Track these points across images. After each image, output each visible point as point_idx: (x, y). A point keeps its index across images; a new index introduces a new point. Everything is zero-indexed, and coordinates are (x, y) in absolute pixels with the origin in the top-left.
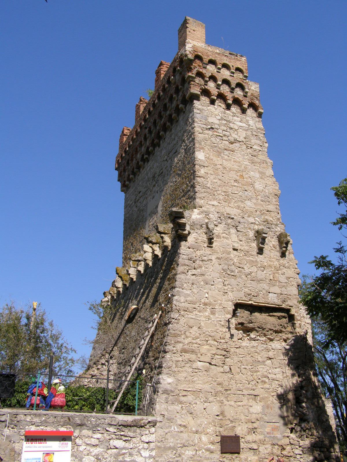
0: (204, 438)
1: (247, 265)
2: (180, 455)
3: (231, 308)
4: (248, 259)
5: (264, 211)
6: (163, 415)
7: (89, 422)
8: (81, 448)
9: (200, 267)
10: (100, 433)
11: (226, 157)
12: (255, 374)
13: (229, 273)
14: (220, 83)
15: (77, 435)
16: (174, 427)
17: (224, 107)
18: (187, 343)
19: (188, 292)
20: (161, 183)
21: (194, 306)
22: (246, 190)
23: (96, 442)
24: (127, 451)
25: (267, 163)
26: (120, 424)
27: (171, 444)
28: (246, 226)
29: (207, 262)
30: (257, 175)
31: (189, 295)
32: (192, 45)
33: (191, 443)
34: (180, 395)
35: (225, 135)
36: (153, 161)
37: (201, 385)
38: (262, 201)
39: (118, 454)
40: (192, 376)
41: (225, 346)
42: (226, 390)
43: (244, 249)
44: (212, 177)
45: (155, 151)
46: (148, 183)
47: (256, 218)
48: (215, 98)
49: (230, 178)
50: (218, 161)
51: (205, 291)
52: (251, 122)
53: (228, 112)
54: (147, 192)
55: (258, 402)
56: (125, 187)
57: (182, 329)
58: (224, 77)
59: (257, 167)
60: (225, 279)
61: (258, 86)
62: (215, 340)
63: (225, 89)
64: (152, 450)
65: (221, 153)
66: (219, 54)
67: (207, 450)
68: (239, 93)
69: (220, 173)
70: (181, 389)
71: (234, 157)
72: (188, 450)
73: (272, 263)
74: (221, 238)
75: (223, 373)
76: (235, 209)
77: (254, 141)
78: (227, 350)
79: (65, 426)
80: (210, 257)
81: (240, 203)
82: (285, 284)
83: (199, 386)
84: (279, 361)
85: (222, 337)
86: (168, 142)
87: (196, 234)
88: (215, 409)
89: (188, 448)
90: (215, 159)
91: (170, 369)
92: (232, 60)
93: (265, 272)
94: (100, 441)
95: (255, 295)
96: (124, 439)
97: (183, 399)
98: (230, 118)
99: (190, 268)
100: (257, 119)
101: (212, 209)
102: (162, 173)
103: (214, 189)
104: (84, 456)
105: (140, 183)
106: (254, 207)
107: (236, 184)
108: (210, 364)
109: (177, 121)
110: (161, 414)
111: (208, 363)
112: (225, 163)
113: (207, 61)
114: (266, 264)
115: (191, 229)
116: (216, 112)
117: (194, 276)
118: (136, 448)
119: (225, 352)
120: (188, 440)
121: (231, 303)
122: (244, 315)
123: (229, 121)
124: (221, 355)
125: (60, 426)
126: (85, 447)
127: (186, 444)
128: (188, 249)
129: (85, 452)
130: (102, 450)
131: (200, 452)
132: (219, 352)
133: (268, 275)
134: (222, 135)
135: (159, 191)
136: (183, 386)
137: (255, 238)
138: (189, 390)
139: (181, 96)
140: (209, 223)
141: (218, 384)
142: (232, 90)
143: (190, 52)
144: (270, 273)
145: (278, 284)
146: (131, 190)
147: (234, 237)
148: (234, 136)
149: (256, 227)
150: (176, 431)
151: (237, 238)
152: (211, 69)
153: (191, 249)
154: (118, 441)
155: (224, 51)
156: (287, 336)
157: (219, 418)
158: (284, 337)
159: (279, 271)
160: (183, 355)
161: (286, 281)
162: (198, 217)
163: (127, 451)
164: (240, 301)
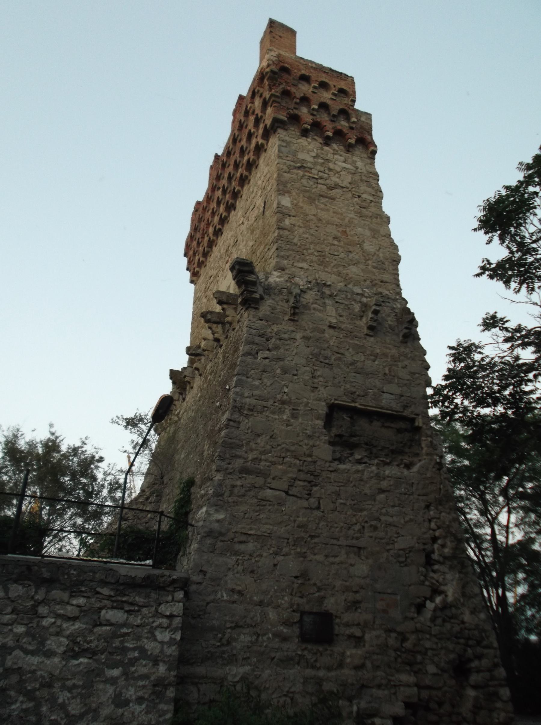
0: (272, 615)
1: (351, 350)
2: (229, 643)
3: (323, 409)
4: (351, 342)
5: (377, 282)
6: (204, 573)
7: (66, 577)
8: (45, 623)
9: (277, 348)
10: (84, 597)
11: (322, 206)
12: (360, 514)
13: (322, 360)
16: (222, 594)
17: (321, 142)
18: (250, 458)
19: (257, 383)
21: (264, 403)
22: (350, 252)
23: (75, 612)
24: (130, 630)
26: (121, 581)
27: (214, 622)
28: (349, 296)
29: (289, 342)
30: (368, 233)
31: (257, 387)
32: (277, 53)
33: (249, 621)
34: (236, 540)
35: (321, 178)
37: (271, 527)
38: (374, 267)
39: (115, 635)
40: (257, 512)
41: (312, 468)
42: (312, 537)
44: (301, 230)
48: (309, 127)
50: (311, 210)
51: (283, 383)
52: (359, 164)
53: (326, 148)
55: (363, 558)
56: (195, 277)
57: (244, 438)
58: (322, 100)
59: (367, 223)
60: (315, 368)
62: (296, 457)
63: (324, 118)
64: (175, 630)
65: (315, 200)
67: (275, 635)
68: (343, 124)
69: (313, 226)
70: (238, 530)
72: (244, 634)
73: (388, 351)
74: (310, 310)
75: (306, 508)
76: (333, 276)
78: (316, 474)
79: (21, 582)
80: (293, 336)
81: (341, 269)
82: (408, 382)
83: (266, 528)
84: (398, 495)
85: (306, 453)
87: (273, 302)
88: (292, 565)
89: (245, 631)
91: (221, 498)
93: (376, 363)
94: (81, 611)
95: (362, 393)
96: (127, 608)
97: (237, 547)
98: (330, 156)
99: (261, 348)
103: (303, 247)
104: (48, 636)
106: (362, 274)
107: (336, 242)
108: (287, 493)
109: (256, 167)
110: (201, 571)
111: (284, 491)
112: (321, 214)
113: (298, 75)
114: (378, 351)
115: (264, 293)
116: (311, 147)
117: (267, 360)
118: (147, 625)
119: (312, 477)
120: (245, 617)
121: (324, 404)
122: (343, 422)
123: (328, 161)
124: (304, 481)
127: (241, 624)
128: (259, 322)
130: (84, 626)
131: (265, 638)
132: (302, 476)
133: (381, 367)
134: (316, 177)
136: (239, 526)
137: (362, 314)
138: (250, 532)
141: (298, 527)
142: (334, 118)
143: (273, 62)
145: (396, 381)
146: (202, 278)
148: (335, 179)
149: (364, 300)
150: (226, 601)
151: (334, 312)
152: (305, 89)
153: (263, 322)
154: (116, 611)
156: (411, 459)
157: (300, 582)
158: (405, 461)
159: (399, 363)
160: (243, 477)
161: (409, 377)
162: (278, 280)
163: (130, 630)
164: (336, 402)
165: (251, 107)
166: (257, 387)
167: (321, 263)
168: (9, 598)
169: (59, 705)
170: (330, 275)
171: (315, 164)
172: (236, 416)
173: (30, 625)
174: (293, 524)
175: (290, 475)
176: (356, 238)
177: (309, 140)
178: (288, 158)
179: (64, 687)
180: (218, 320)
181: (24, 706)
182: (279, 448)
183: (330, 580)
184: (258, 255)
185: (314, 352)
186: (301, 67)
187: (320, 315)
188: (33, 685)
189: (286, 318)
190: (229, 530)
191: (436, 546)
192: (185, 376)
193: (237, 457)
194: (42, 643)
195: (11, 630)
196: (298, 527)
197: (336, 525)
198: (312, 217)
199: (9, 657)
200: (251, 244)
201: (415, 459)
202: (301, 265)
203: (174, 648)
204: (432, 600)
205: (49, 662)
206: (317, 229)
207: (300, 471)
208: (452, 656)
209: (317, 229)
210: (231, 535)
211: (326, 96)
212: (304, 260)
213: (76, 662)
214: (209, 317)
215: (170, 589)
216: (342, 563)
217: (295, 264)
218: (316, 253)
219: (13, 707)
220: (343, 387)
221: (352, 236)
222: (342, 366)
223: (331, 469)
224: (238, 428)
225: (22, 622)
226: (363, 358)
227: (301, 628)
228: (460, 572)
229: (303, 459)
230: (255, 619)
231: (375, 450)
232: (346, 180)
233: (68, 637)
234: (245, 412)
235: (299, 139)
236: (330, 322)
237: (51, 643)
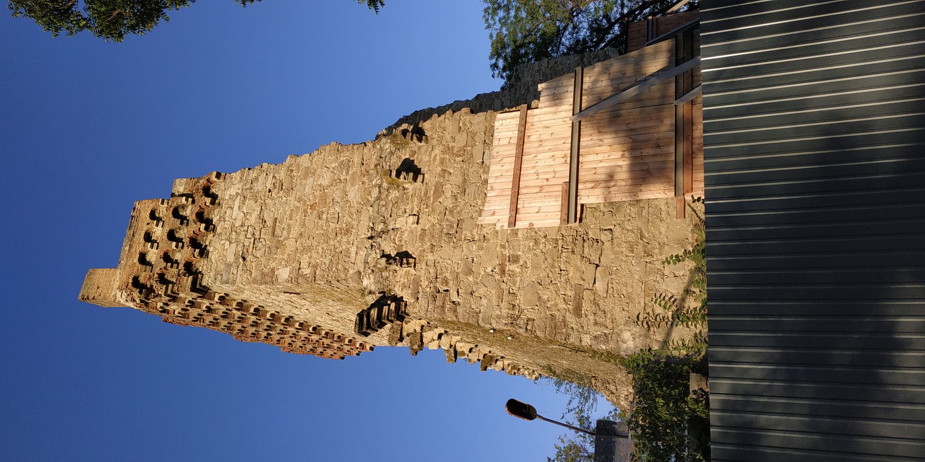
1: (440, 200)
11: (285, 232)
14: (174, 244)
18: (565, 306)
21: (506, 292)
30: (310, 181)
31: (490, 301)
38: (347, 173)
41: (570, 239)
43: (417, 206)
44: (314, 255)
48: (197, 251)
50: (291, 245)
51: (482, 273)
52: (232, 191)
53: (219, 230)
66: (131, 246)
73: (438, 158)
77: (258, 187)
78: (575, 234)
90: (288, 251)
98: (227, 225)
100: (228, 180)
103: (333, 253)
107: (324, 216)
108: (597, 266)
112: (294, 233)
114: (439, 169)
123: (233, 225)
132: (578, 249)
138: (643, 304)
148: (253, 219)
153: (420, 296)
161: (465, 134)
166: (490, 301)
167: (348, 231)
171: (238, 242)
172: (521, 322)
176: (318, 193)
182: (551, 275)
186: (130, 263)
187: (406, 234)
189: (412, 270)
196: (632, 251)
197: (628, 211)
200: (331, 302)
202: (353, 255)
211: (159, 232)
212: (348, 250)
214: (416, 347)
221: (315, 197)
222: (459, 209)
229: (560, 248)
236: (413, 223)
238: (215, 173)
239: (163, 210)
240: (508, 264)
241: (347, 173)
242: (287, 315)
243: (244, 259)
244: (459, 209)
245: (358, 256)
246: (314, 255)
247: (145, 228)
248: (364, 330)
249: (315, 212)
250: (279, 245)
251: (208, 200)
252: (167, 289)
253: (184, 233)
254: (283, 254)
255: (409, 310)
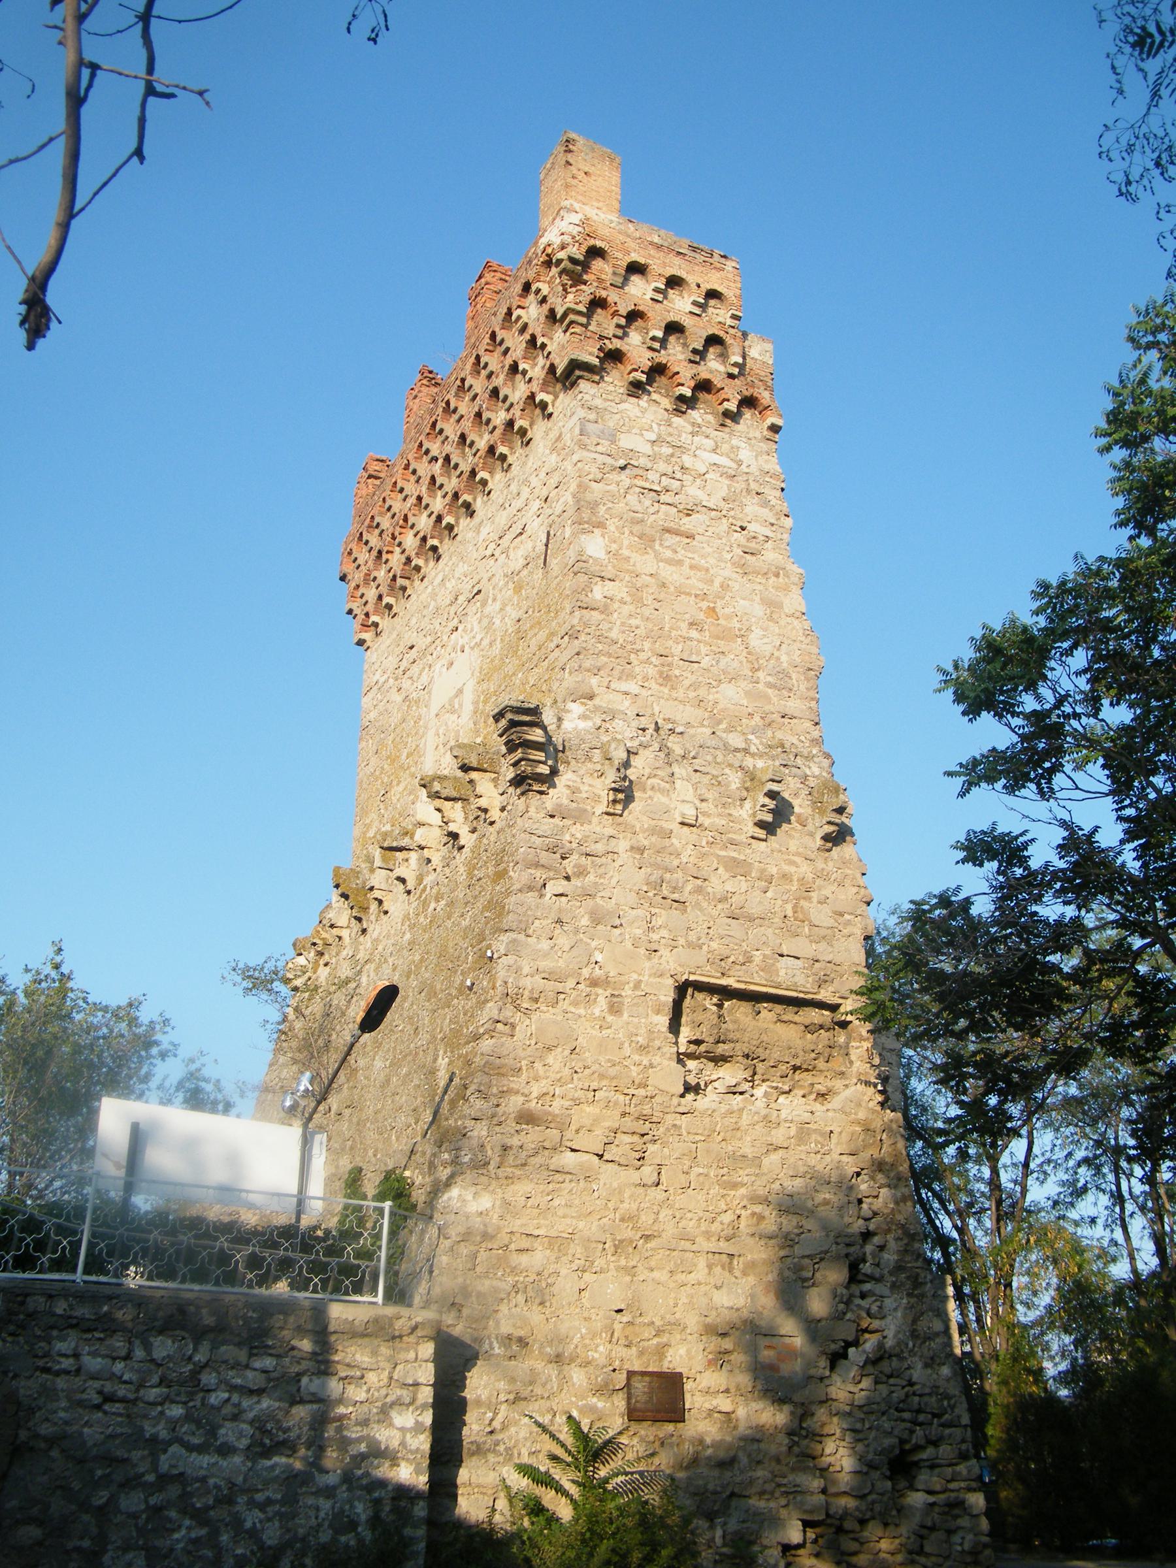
1: (721, 870)
4: (723, 853)
7: (241, 1323)
8: (214, 1399)
9: (582, 872)
10: (271, 1355)
11: (668, 554)
12: (733, 1193)
13: (665, 893)
14: (660, 334)
15: (203, 1360)
17: (669, 407)
18: (535, 1095)
20: (475, 623)
21: (560, 987)
25: (787, 576)
29: (604, 859)
30: (759, 610)
32: (580, 216)
34: (513, 1247)
36: (454, 559)
37: (574, 1222)
38: (770, 685)
40: (548, 1194)
41: (647, 1110)
42: (647, 1238)
43: (712, 824)
44: (626, 609)
45: (461, 527)
46: (436, 623)
47: (751, 737)
48: (644, 378)
49: (678, 617)
50: (645, 563)
51: (594, 944)
52: (745, 454)
53: (677, 421)
54: (434, 646)
60: (654, 911)
61: (769, 347)
66: (659, 247)
71: (690, 555)
73: (793, 869)
76: (688, 708)
77: (752, 507)
78: (654, 1119)
79: (171, 1333)
86: (501, 501)
90: (635, 557)
92: (696, 268)
94: (269, 1380)
98: (686, 438)
100: (765, 446)
101: (625, 704)
102: (479, 592)
103: (629, 647)
105: (414, 621)
107: (694, 634)
108: (601, 1156)
114: (774, 870)
117: (563, 898)
125: (153, 1333)
126: (226, 1395)
129: (228, 1410)
133: (779, 902)
134: (658, 489)
135: (467, 649)
136: (518, 1222)
137: (745, 793)
138: (536, 1233)
139: (543, 367)
140: (613, 745)
141: (622, 1220)
143: (574, 237)
144: (785, 897)
145: (807, 929)
147: (684, 789)
148: (694, 492)
149: (749, 762)
153: (556, 820)
155: (675, 239)
156: (829, 1084)
157: (625, 1319)
159: (812, 894)
162: (582, 725)
164: (692, 978)
165: (519, 318)
166: (546, 955)
167: (666, 678)
168: (152, 1361)
169: (247, 1532)
170: (681, 707)
171: (653, 458)
172: (508, 1013)
173: (191, 1404)
174: (612, 1216)
175: (607, 1124)
176: (735, 624)
177: (641, 402)
178: (600, 448)
179: (252, 1504)
180: (454, 794)
181: (193, 1535)
182: (587, 1071)
183: (677, 1316)
184: (533, 648)
185: (653, 878)
186: (631, 244)
187: (664, 800)
188: (204, 1500)
189: (602, 807)
190: (499, 1229)
191: (869, 1248)
192: (372, 889)
193: (510, 1091)
194: (213, 1432)
195: (162, 1413)
196: (622, 1220)
197: (689, 1215)
198: (648, 578)
199: (163, 1457)
200: (515, 615)
201: (838, 1084)
203: (422, 1437)
204: (856, 1343)
205: (225, 1464)
206: (657, 605)
207: (624, 1114)
208: (887, 1442)
209: (657, 605)
210: (504, 1238)
211: (680, 305)
212: (631, 676)
213: (269, 1463)
214: (437, 786)
215: (412, 1339)
216: (699, 1284)
217: (613, 686)
218: (653, 659)
219: (176, 1536)
220: (705, 948)
221: (728, 618)
222: (705, 904)
223: (681, 1110)
224: (512, 1036)
225: (178, 1399)
226: (744, 886)
227: (629, 1398)
228: (909, 1295)
229: (631, 1091)
230: (548, 1387)
231: (761, 1068)
232: (716, 491)
233: (251, 1423)
234: (525, 1005)
235: (622, 401)
236: (683, 815)
237: (227, 1433)
238: (779, 422)
239: (719, 315)
240: (608, 993)
241: (770, 685)
242: (479, 504)
243: (623, 468)
244: (705, 904)
245: (621, 697)
246: (626, 609)
247: (691, 279)
248: (509, 716)
249: (702, 616)
250: (647, 541)
251: (732, 406)
252: (579, 313)
253: (675, 355)
254: (630, 547)
255: (534, 799)
